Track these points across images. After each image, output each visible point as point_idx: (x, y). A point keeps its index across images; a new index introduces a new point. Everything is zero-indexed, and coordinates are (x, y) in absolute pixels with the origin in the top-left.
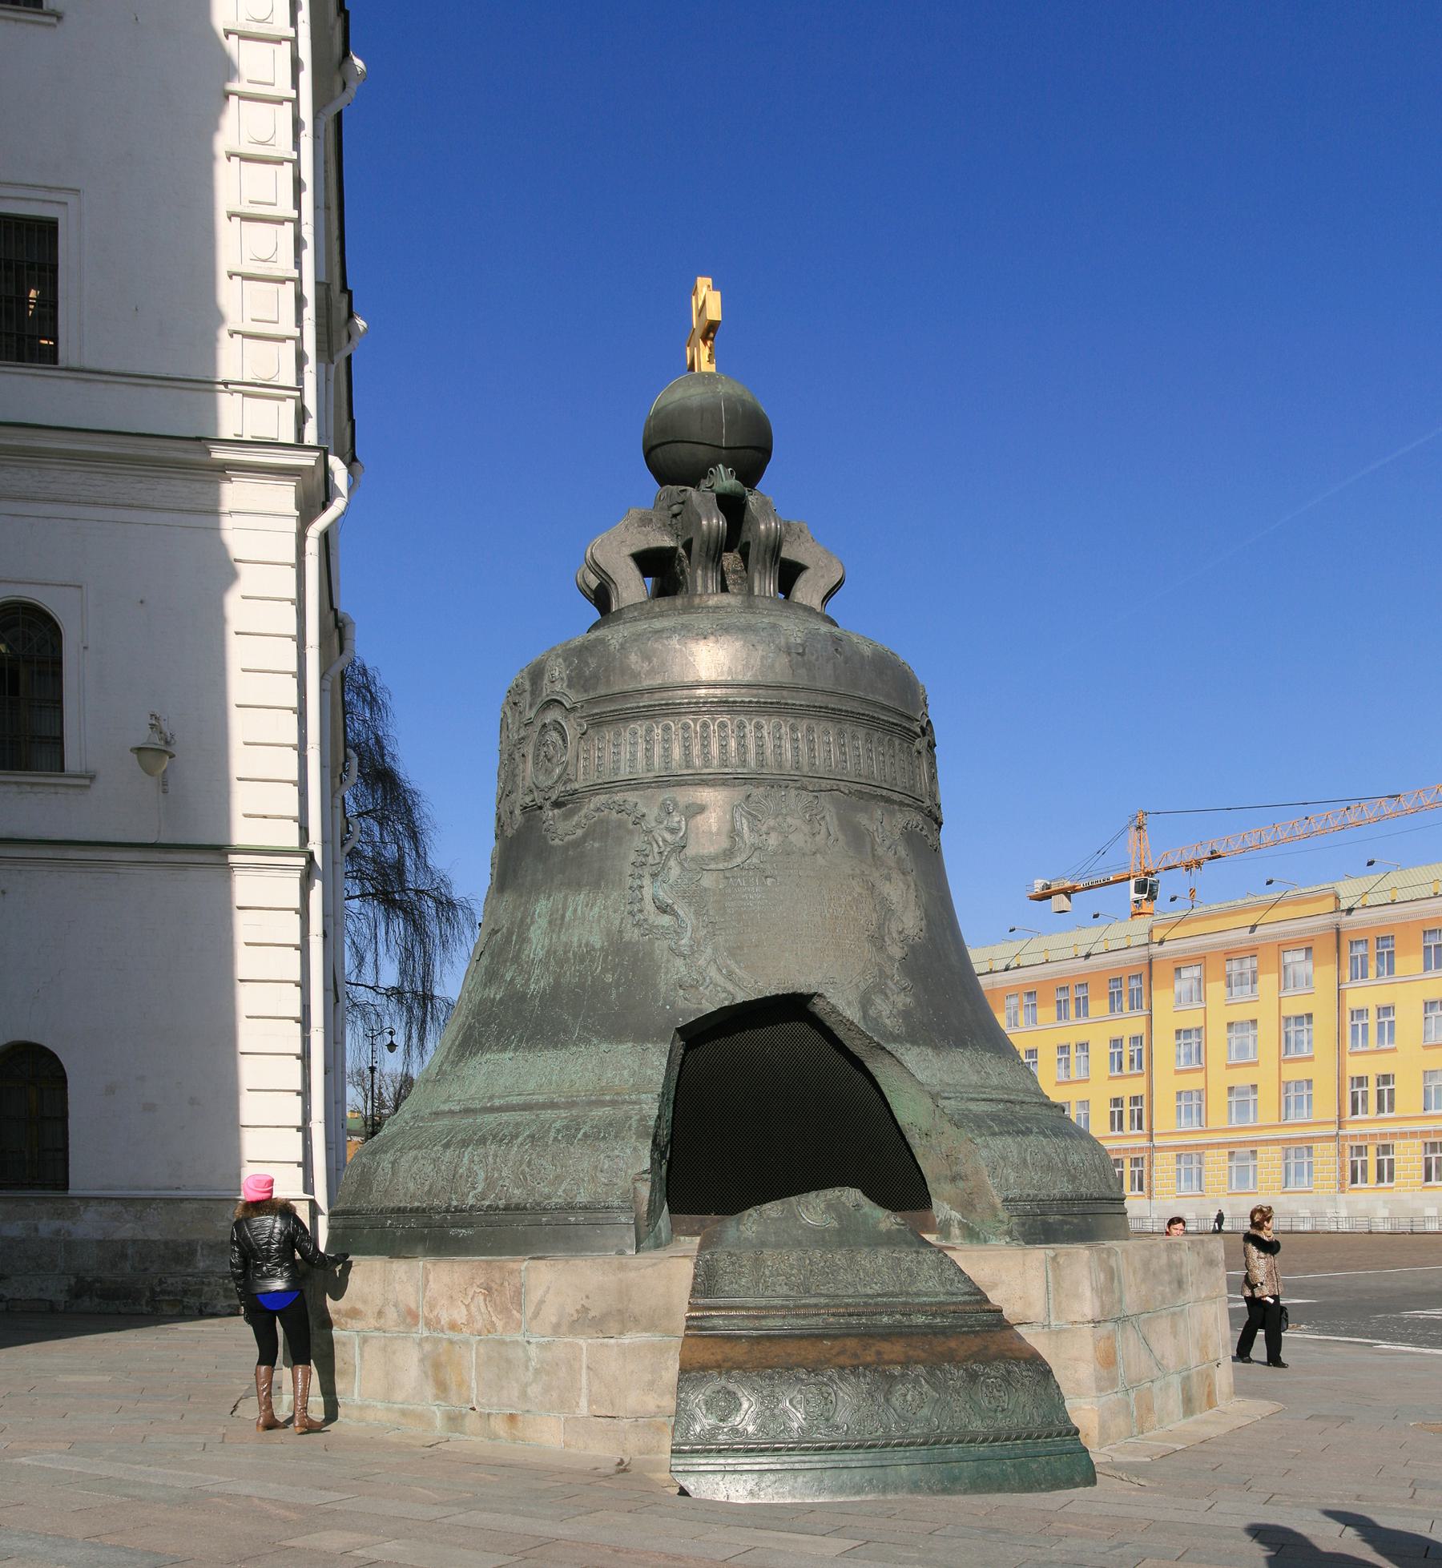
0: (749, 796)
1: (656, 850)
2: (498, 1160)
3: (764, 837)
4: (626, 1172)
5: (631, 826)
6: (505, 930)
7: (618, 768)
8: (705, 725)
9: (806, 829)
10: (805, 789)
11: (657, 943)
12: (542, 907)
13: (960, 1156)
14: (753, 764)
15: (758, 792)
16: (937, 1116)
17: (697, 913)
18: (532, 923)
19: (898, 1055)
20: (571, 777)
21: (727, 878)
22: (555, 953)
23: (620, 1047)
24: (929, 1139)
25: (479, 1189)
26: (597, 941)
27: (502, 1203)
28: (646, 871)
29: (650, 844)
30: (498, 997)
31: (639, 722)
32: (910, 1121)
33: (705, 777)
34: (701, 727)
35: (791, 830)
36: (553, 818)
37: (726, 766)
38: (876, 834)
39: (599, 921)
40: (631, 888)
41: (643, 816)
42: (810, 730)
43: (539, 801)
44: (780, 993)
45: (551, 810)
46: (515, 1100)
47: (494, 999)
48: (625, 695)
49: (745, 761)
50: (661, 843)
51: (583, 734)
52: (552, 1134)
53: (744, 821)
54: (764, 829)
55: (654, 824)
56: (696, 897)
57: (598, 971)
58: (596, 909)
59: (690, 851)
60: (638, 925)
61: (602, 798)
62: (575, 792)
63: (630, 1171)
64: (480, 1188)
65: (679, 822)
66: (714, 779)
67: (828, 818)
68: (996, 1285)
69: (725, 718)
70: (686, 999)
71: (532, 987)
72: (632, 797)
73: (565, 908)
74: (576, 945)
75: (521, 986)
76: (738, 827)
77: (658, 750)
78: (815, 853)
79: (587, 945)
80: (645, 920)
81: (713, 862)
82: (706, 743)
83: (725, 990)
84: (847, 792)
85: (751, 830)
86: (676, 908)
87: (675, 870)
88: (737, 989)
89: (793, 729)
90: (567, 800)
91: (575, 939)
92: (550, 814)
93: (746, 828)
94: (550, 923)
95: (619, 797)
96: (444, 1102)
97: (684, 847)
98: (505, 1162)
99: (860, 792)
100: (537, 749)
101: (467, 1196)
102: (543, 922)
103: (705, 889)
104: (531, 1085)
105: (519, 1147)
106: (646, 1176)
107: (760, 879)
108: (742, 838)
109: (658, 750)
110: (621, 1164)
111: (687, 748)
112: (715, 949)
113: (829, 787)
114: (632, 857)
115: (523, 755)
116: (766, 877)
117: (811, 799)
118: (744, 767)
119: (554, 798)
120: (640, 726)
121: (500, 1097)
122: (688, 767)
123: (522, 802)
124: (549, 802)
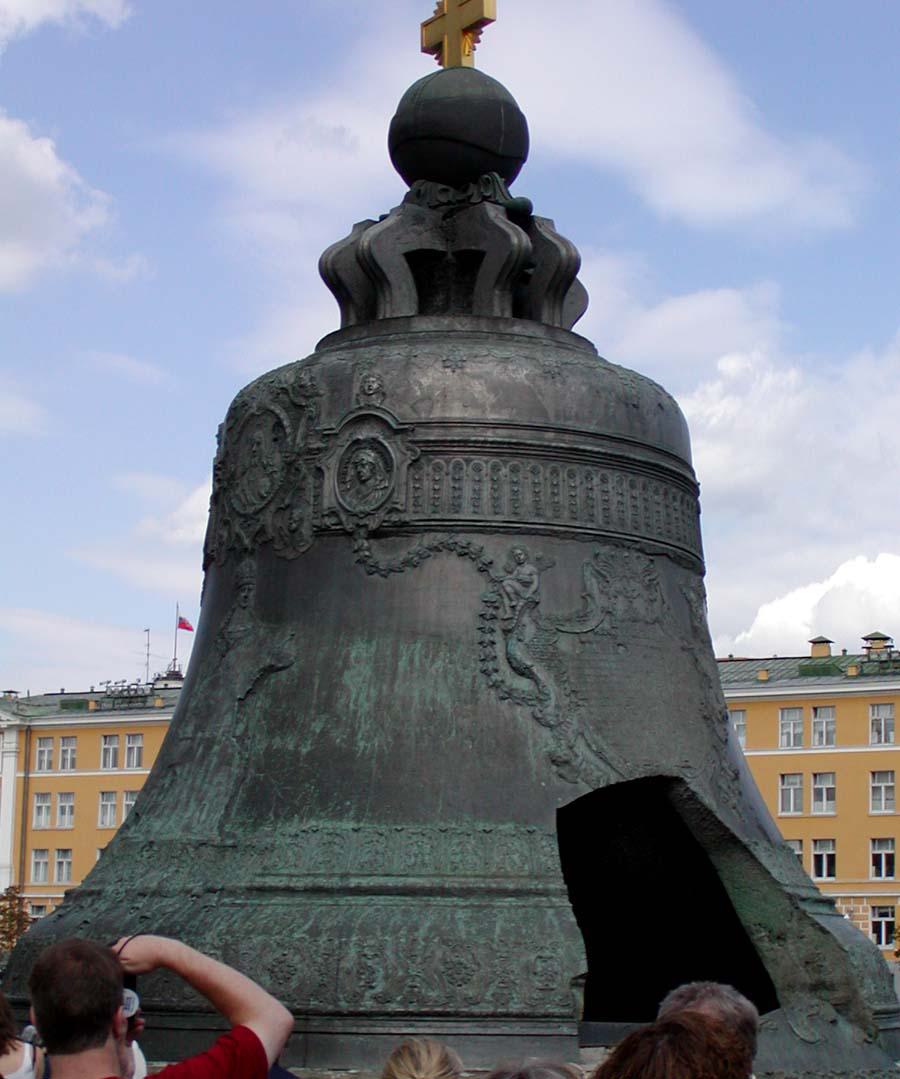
1: (506, 601)
2: (401, 955)
3: (613, 599)
4: (562, 975)
5: (476, 575)
6: (294, 668)
7: (459, 506)
8: (554, 472)
9: (645, 594)
11: (519, 709)
12: (359, 650)
13: (826, 964)
14: (600, 519)
15: (604, 550)
16: (795, 918)
17: (557, 679)
18: (346, 666)
19: (751, 848)
20: (398, 506)
21: (582, 642)
22: (389, 707)
23: (501, 827)
24: (782, 943)
25: (379, 989)
26: (443, 696)
27: (411, 1008)
28: (497, 626)
29: (500, 595)
30: (304, 751)
31: (485, 458)
32: (757, 921)
33: (556, 528)
34: (552, 473)
35: (635, 594)
36: (368, 549)
37: (575, 519)
39: (445, 677)
40: (481, 643)
41: (491, 563)
42: (644, 488)
43: (349, 527)
44: (648, 775)
45: (367, 539)
46: (391, 882)
47: (296, 753)
48: (463, 423)
49: (592, 515)
50: (512, 596)
51: (414, 461)
52: (461, 926)
53: (594, 580)
54: (612, 591)
55: (502, 573)
56: (552, 659)
57: (454, 734)
58: (439, 663)
59: (541, 607)
60: (495, 686)
61: (441, 536)
62: (405, 524)
63: (566, 974)
64: (380, 987)
65: (531, 575)
66: (566, 532)
69: (575, 467)
70: (561, 776)
71: (362, 744)
72: (478, 541)
73: (396, 656)
74: (416, 700)
75: (343, 740)
76: (588, 587)
77: (506, 489)
79: (433, 701)
80: (502, 682)
81: (568, 624)
82: (556, 491)
83: (599, 770)
84: (672, 556)
85: (602, 592)
86: (534, 669)
87: (530, 631)
88: (609, 767)
89: (632, 486)
90: (392, 532)
91: (416, 694)
92: (366, 544)
93: (595, 586)
94: (376, 670)
95: (462, 539)
96: (262, 875)
97: (537, 603)
98: (412, 957)
100: (344, 463)
101: (362, 996)
102: (367, 671)
103: (564, 654)
104: (397, 866)
105: (424, 940)
106: (582, 981)
107: (613, 647)
108: (593, 598)
109: (506, 489)
110: (557, 968)
111: (537, 494)
112: (581, 721)
113: (660, 551)
114: (480, 608)
115: (319, 470)
116: (619, 645)
117: (648, 563)
118: (593, 521)
119: (373, 524)
120: (486, 462)
121: (356, 876)
122: (538, 515)
123: (317, 522)
124: (362, 532)
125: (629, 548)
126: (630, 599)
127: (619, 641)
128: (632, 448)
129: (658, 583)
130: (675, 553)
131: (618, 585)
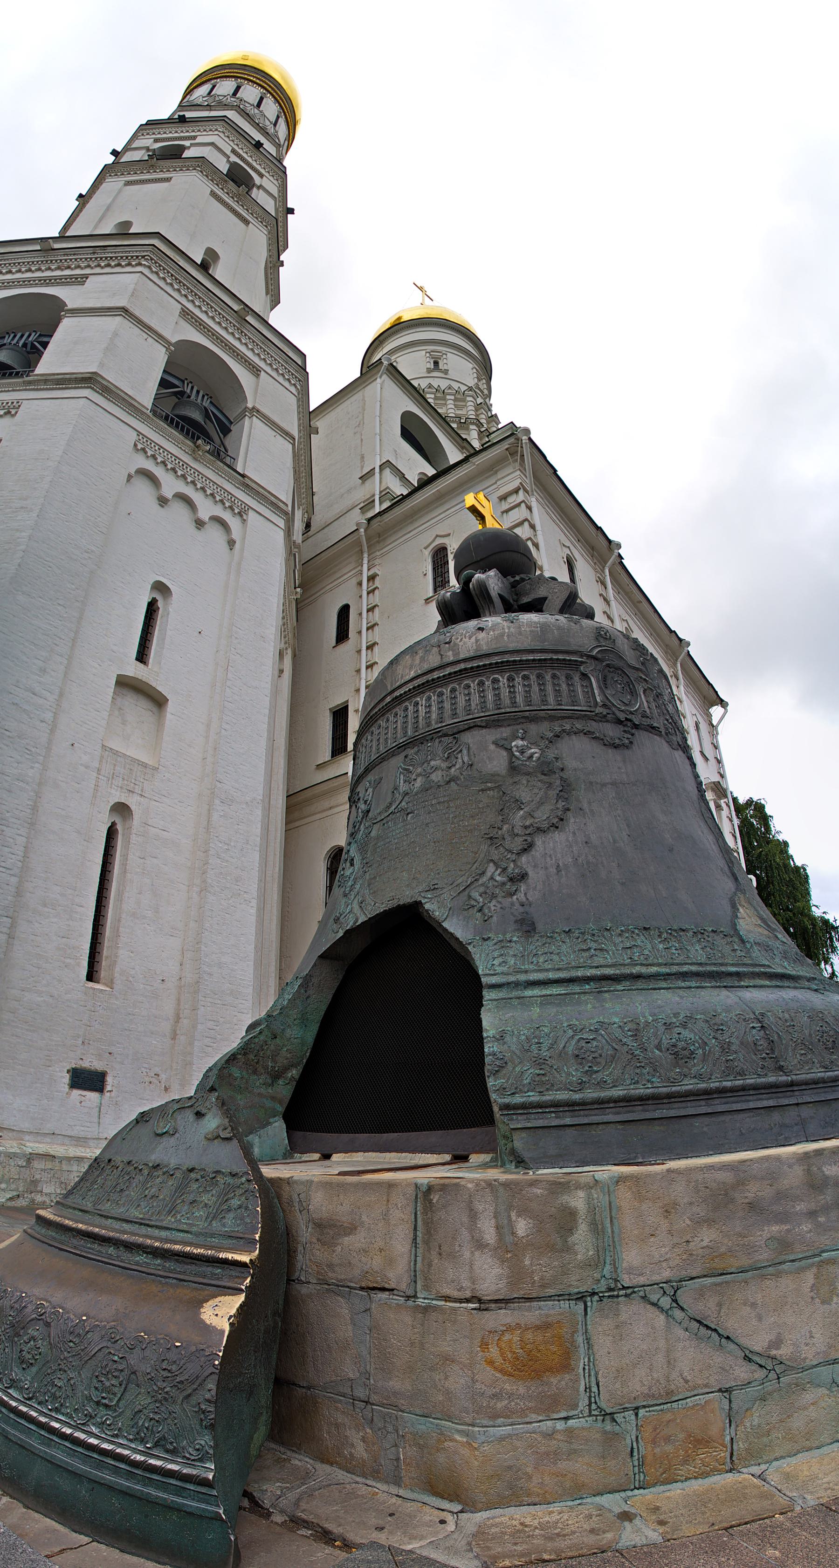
0: (406, 757)
9: (444, 765)
10: (446, 735)
15: (411, 752)
38: (514, 749)
53: (402, 776)
54: (414, 777)
59: (370, 814)
67: (465, 752)
68: (356, 1228)
78: (448, 782)
84: (484, 724)
85: (405, 781)
93: (402, 781)
99: (498, 720)
113: (466, 727)
116: (408, 814)
125: (432, 739)
126: (427, 775)
127: (409, 811)
128: (442, 671)
129: (461, 751)
130: (486, 720)
131: (419, 770)
